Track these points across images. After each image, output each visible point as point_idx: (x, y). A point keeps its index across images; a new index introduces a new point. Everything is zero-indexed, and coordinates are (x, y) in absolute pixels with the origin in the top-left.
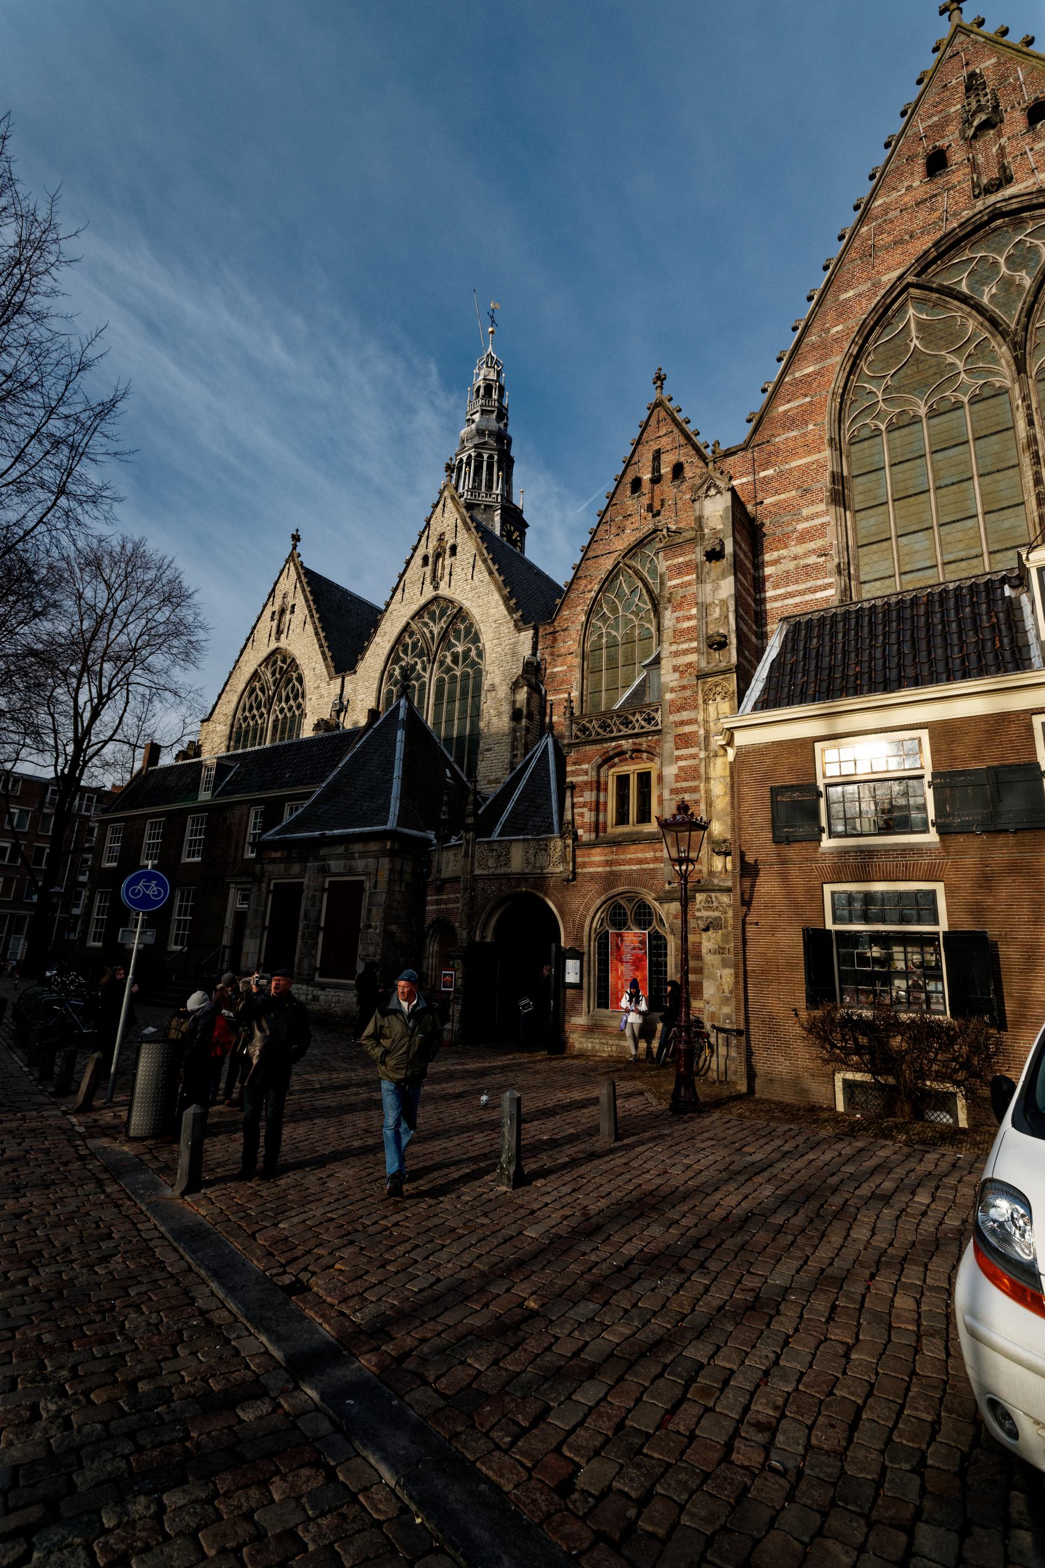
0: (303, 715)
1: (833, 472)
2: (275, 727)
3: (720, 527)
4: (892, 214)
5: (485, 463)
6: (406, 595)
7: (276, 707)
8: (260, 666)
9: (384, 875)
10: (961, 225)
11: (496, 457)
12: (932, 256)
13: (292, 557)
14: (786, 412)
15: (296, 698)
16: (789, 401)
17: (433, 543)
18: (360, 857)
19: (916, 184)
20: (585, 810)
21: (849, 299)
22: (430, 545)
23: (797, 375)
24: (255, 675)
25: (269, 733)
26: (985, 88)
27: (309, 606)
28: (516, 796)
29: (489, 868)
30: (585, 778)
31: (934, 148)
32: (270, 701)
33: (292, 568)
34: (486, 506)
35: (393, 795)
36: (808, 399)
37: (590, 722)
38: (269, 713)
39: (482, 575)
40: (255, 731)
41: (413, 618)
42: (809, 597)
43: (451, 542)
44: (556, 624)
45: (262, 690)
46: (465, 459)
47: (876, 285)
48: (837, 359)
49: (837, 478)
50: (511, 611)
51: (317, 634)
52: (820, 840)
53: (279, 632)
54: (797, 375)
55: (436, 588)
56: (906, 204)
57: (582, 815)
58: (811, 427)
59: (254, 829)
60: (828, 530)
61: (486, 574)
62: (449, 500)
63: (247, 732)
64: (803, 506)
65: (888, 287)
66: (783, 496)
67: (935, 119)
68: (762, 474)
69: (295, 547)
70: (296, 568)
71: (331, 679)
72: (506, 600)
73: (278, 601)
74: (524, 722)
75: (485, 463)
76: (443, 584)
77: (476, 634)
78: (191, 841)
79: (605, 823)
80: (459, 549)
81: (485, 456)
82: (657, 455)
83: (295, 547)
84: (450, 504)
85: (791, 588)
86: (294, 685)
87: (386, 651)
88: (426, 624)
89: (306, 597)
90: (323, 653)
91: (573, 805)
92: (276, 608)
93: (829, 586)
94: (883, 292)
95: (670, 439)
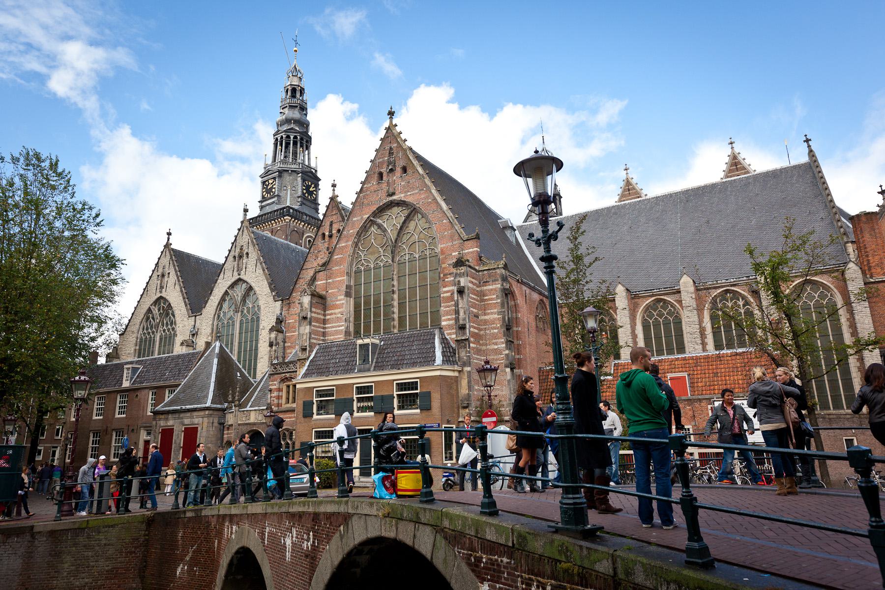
0: (175, 335)
2: (161, 339)
7: (160, 329)
8: (151, 305)
9: (205, 425)
11: (299, 137)
13: (167, 246)
17: (238, 250)
18: (196, 418)
24: (149, 310)
25: (157, 344)
27: (177, 275)
28: (258, 390)
30: (275, 387)
32: (157, 326)
33: (167, 252)
34: (292, 171)
35: (210, 390)
38: (157, 332)
39: (260, 271)
40: (150, 341)
41: (228, 288)
42: (338, 329)
43: (246, 251)
45: (153, 318)
46: (279, 138)
48: (350, 243)
49: (348, 287)
50: (272, 290)
51: (182, 291)
52: (312, 417)
53: (162, 287)
55: (239, 275)
57: (274, 401)
59: (152, 401)
60: (344, 306)
62: (245, 228)
63: (145, 341)
68: (329, 281)
69: (168, 240)
70: (170, 252)
71: (189, 317)
72: (270, 285)
73: (161, 270)
75: (292, 142)
76: (242, 272)
78: (120, 406)
79: (282, 403)
81: (292, 137)
82: (331, 225)
83: (168, 240)
84: (246, 231)
85: (334, 325)
86: (170, 317)
87: (216, 304)
89: (175, 269)
90: (185, 302)
91: (271, 397)
92: (159, 273)
93: (343, 325)
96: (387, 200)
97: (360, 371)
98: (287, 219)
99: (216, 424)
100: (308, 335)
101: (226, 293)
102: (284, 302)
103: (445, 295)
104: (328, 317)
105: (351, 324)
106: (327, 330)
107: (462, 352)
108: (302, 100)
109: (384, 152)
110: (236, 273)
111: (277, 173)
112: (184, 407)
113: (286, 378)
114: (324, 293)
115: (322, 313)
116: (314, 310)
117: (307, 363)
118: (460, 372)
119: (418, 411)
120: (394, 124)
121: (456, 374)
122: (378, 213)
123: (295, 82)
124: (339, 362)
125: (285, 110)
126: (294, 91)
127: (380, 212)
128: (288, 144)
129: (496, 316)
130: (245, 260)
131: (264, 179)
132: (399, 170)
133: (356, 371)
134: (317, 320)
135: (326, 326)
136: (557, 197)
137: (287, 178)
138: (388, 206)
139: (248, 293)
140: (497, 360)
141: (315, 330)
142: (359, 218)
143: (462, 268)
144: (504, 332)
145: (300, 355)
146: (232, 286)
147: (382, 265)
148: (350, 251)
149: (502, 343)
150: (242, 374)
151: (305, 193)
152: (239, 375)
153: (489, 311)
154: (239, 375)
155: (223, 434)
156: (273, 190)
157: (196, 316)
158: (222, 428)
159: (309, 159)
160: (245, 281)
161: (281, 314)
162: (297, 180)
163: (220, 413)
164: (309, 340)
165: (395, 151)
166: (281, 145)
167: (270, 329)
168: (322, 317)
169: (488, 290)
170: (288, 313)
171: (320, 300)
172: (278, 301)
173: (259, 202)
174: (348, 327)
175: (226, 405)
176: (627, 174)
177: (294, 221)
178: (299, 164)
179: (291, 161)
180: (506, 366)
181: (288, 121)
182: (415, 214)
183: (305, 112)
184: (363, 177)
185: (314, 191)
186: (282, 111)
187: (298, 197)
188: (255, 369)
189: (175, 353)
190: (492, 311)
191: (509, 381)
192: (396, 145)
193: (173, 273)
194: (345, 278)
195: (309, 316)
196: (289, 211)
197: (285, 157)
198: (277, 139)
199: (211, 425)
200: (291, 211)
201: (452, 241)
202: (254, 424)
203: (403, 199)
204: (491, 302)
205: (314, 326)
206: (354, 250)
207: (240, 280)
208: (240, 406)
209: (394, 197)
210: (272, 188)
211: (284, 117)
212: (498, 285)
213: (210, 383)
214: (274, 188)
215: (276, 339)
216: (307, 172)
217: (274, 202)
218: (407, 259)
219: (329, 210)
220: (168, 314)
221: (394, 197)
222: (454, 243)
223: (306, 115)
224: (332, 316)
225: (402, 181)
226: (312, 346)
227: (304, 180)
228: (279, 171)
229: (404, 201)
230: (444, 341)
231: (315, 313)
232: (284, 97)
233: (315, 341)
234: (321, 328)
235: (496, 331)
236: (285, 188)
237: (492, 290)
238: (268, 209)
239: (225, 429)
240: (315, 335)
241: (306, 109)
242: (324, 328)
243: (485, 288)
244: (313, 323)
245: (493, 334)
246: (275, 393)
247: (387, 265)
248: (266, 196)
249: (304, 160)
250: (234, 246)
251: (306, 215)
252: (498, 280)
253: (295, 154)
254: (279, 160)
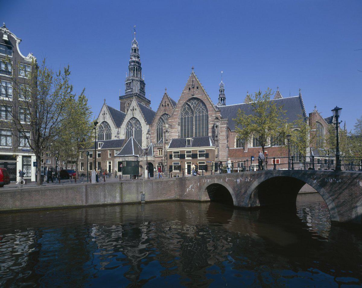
4: (185, 94)
7: (105, 131)
15: (109, 130)
27: (110, 114)
40: (102, 135)
50: (145, 122)
72: (145, 120)
77: (140, 124)
80: (137, 110)
81: (136, 68)
82: (165, 102)
88: (132, 121)
97: (187, 147)
101: (129, 121)
112: (125, 155)
118: (215, 148)
119: (205, 158)
121: (214, 149)
126: (135, 50)
129: (225, 134)
150: (139, 147)
166: (132, 70)
180: (227, 147)
189: (112, 140)
193: (108, 114)
207: (133, 117)
209: (194, 96)
220: (107, 127)
227: (140, 84)
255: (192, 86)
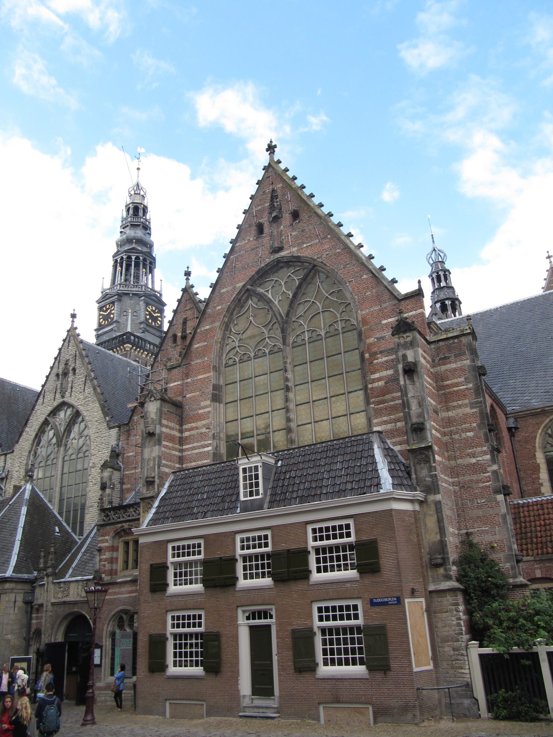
1: (213, 384)
3: (155, 418)
4: (243, 252)
5: (133, 263)
6: (46, 400)
10: (266, 265)
11: (141, 258)
12: (256, 278)
14: (197, 348)
16: (198, 343)
17: (62, 366)
19: (251, 239)
20: (106, 563)
21: (224, 293)
22: (61, 367)
23: (203, 329)
26: (277, 199)
28: (83, 550)
29: (59, 598)
30: (106, 544)
31: (259, 222)
34: (133, 294)
36: (206, 343)
37: (110, 512)
39: (89, 390)
41: (49, 415)
44: (130, 425)
46: (119, 260)
47: (234, 288)
48: (217, 324)
49: (216, 387)
50: (105, 414)
54: (203, 329)
55: (63, 397)
56: (247, 248)
57: (104, 566)
58: (206, 359)
60: (211, 415)
61: (92, 389)
64: (202, 401)
65: (238, 291)
66: (193, 394)
67: (260, 207)
74: (108, 491)
75: (133, 263)
79: (116, 570)
80: (77, 371)
81: (133, 258)
82: (185, 323)
85: (196, 444)
91: (101, 560)
94: (236, 293)
95: (192, 312)
96: (272, 259)
97: (244, 510)
98: (128, 347)
99: (20, 604)
100: (157, 459)
101: (46, 423)
102: (122, 428)
103: (376, 385)
104: (187, 434)
105: (222, 442)
106: (185, 454)
107: (422, 469)
108: (146, 220)
109: (265, 196)
110: (58, 395)
111: (116, 297)
113: (124, 530)
114: (180, 398)
115: (178, 427)
116: (164, 422)
117: (156, 504)
118: (421, 503)
120: (276, 160)
122: (258, 279)
123: (138, 200)
124: (208, 498)
125: (126, 229)
126: (136, 209)
127: (261, 277)
128: (128, 266)
129: (468, 410)
130: (71, 378)
131: (101, 304)
132: (287, 218)
133: (238, 511)
134: (171, 438)
135: (184, 447)
136: (457, 302)
137: (127, 301)
138: (274, 266)
139: (75, 420)
140: (478, 481)
141: (168, 454)
142: (230, 288)
143: (408, 334)
144: (486, 435)
145: (145, 491)
146: (54, 412)
147: (267, 352)
148: (219, 335)
149: (485, 453)
151: (149, 319)
152: (57, 529)
153: (455, 404)
154: (57, 529)
155: (31, 619)
156: (112, 316)
157: (6, 455)
158: (29, 609)
159: (153, 282)
160: (70, 406)
161: (118, 445)
162: (139, 304)
163: (27, 587)
164: (159, 468)
165: (279, 193)
166: (122, 267)
167: (102, 466)
168: (178, 434)
169: (450, 371)
170: (128, 444)
171: (173, 409)
172: (113, 427)
173: (95, 330)
174: (217, 448)
175: (36, 573)
176: (551, 262)
177: (135, 350)
178: (142, 286)
179: (132, 283)
181: (129, 241)
182: (314, 275)
183: (148, 231)
184: (234, 233)
185: (159, 317)
186: (122, 230)
187: (141, 323)
188: (82, 523)
190: (460, 403)
191: (504, 517)
192: (280, 185)
194: (211, 374)
195: (158, 431)
196: (128, 338)
197: (126, 280)
198: (116, 261)
199: (12, 605)
200: (132, 338)
201: (380, 302)
202: (75, 603)
203: (295, 255)
204: (455, 389)
205: (166, 447)
206: (224, 334)
208: (56, 575)
209: (283, 254)
210: (110, 313)
211: (124, 236)
212: (465, 362)
213: (14, 541)
214: (113, 314)
215: (110, 478)
216: (150, 295)
217: (112, 330)
218: (307, 339)
219: (181, 305)
221: (283, 254)
222: (384, 305)
223: (150, 234)
224: (192, 432)
225: (294, 230)
226: (163, 477)
227: (147, 304)
228: (118, 294)
229: (299, 257)
230: (388, 452)
231: (167, 427)
232: (125, 216)
233: (167, 470)
234: (176, 450)
235: (470, 434)
236: (125, 313)
237: (455, 369)
238: (105, 338)
239: (34, 611)
240: (167, 461)
241: (150, 228)
242: (181, 451)
243: (443, 368)
244: (164, 443)
245: (466, 439)
246: (107, 553)
247: (276, 349)
248: (103, 323)
249: (147, 284)
250: (57, 362)
251: (150, 343)
252: (464, 354)
253: (137, 277)
254: (119, 283)
255: (270, 213)
